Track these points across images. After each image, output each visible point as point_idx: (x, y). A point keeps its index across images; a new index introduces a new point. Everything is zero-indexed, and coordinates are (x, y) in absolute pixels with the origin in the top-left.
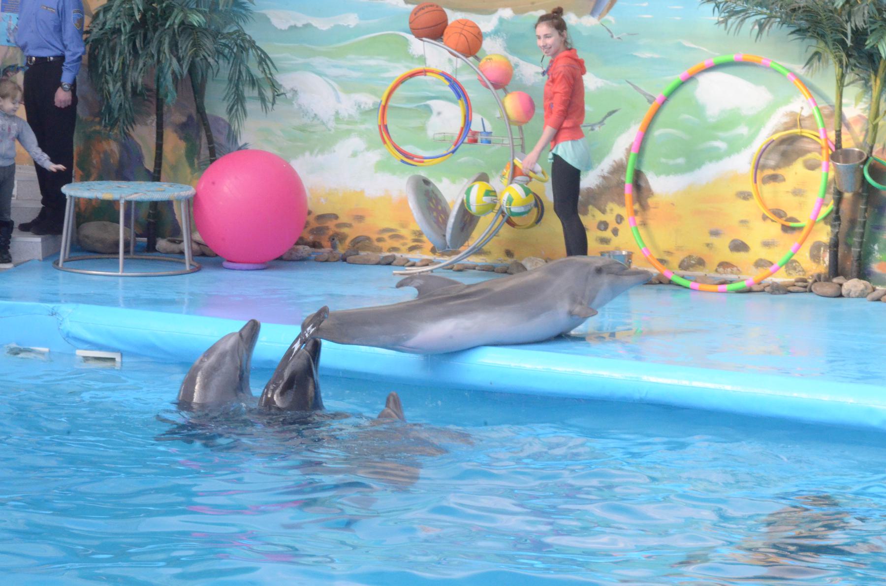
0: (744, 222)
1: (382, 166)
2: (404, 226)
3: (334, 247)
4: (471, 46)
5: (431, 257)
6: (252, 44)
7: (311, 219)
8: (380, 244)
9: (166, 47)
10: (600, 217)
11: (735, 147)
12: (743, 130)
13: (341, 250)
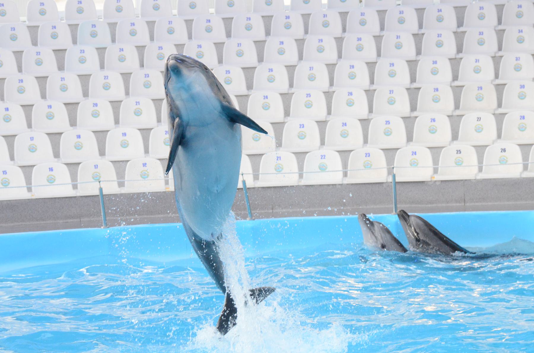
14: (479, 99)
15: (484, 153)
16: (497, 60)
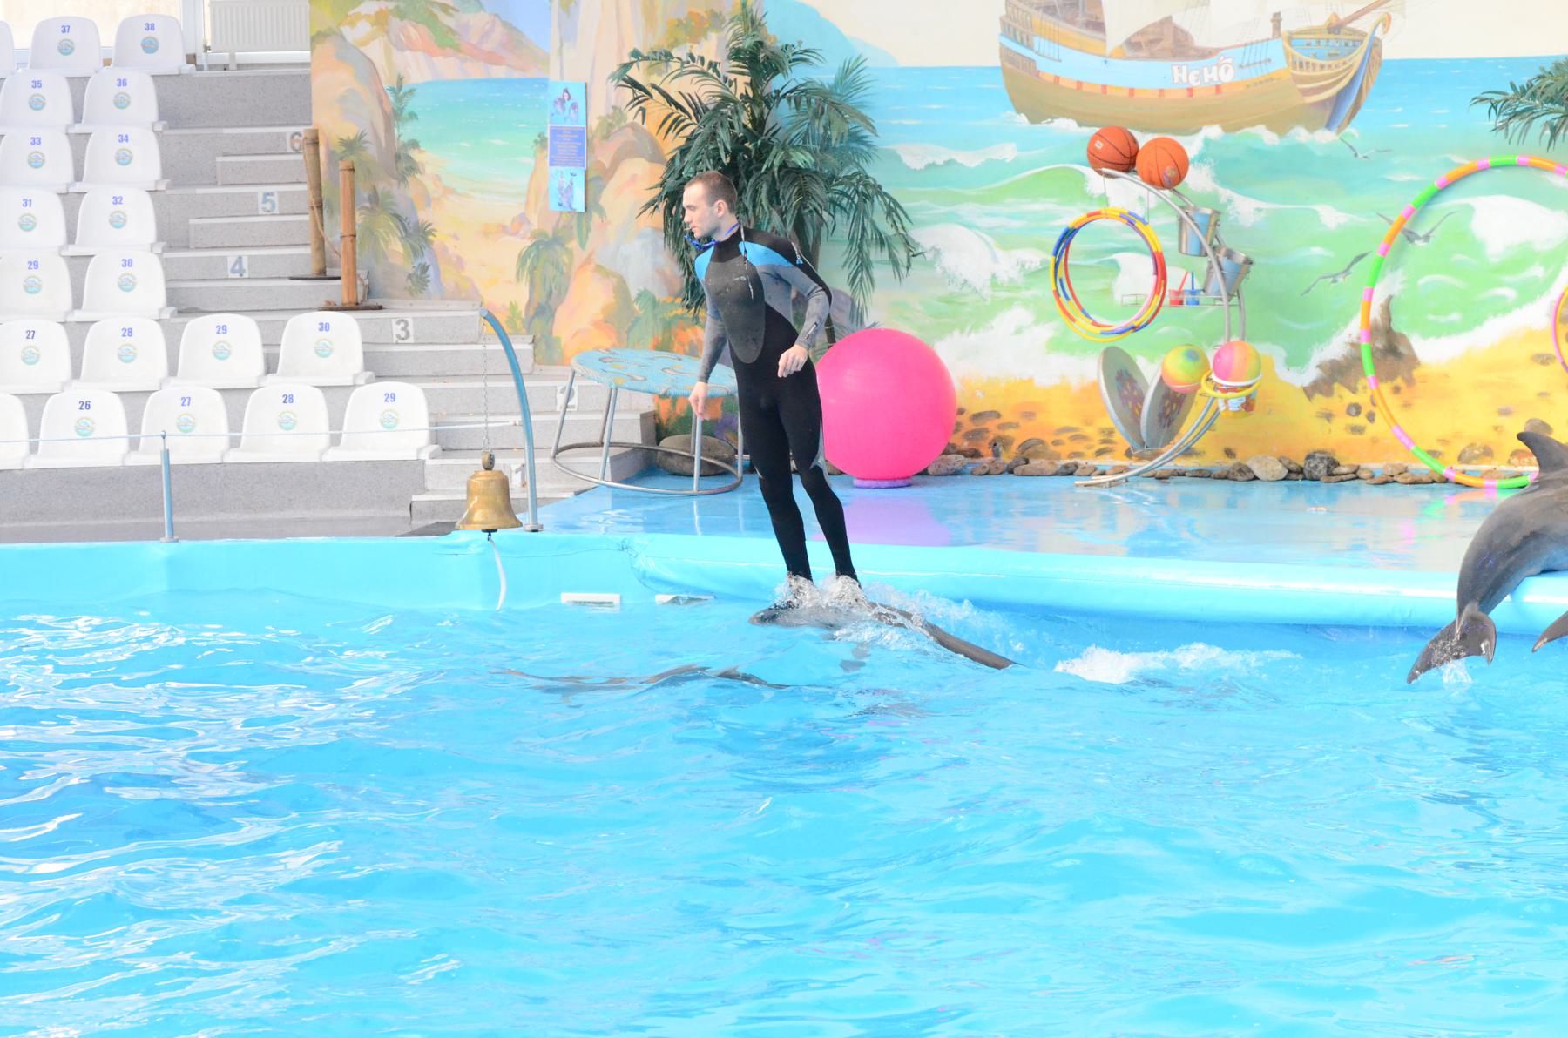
0: (1542, 394)
1: (1055, 345)
2: (1088, 423)
3: (996, 455)
4: (1170, 176)
5: (1126, 462)
6: (878, 190)
7: (964, 419)
8: (1058, 449)
9: (763, 197)
10: (1350, 398)
11: (1528, 293)
12: (1537, 271)
13: (1006, 459)
14: (32, 288)
15: (41, 410)
16: (71, 202)
